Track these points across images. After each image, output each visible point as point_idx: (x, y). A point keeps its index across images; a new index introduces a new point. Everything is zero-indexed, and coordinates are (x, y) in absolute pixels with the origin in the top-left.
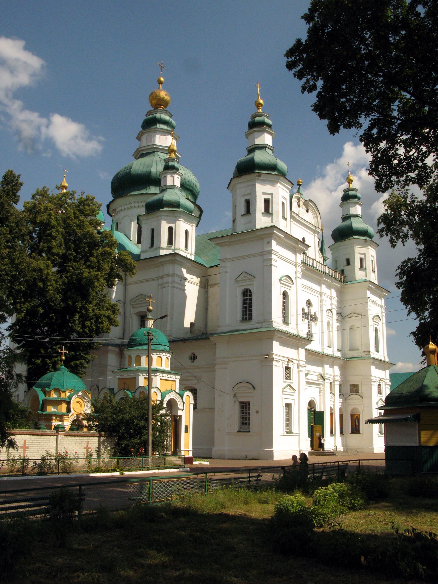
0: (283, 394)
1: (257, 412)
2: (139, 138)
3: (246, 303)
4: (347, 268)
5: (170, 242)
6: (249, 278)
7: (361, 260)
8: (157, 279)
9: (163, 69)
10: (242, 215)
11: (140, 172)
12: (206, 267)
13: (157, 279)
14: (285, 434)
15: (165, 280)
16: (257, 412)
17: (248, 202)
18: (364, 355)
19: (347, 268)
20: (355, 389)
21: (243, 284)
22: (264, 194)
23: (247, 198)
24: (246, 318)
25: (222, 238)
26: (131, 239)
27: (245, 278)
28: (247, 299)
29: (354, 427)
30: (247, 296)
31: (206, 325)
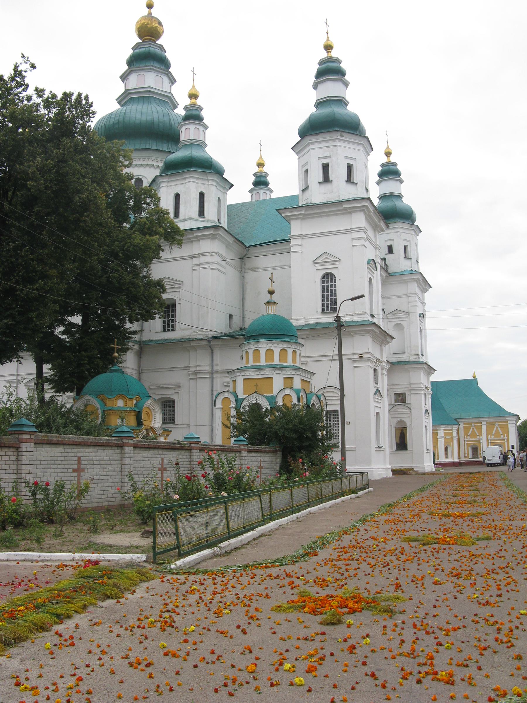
0: (375, 401)
2: (124, 77)
3: (327, 291)
4: (389, 257)
5: (202, 213)
6: (333, 260)
7: (405, 247)
8: (191, 258)
10: (320, 183)
11: (137, 122)
12: (245, 246)
13: (191, 258)
14: (377, 449)
15: (203, 259)
17: (326, 167)
18: (412, 359)
19: (389, 257)
20: (400, 398)
22: (346, 157)
23: (325, 161)
24: (328, 309)
25: (295, 209)
28: (327, 286)
31: (243, 318)
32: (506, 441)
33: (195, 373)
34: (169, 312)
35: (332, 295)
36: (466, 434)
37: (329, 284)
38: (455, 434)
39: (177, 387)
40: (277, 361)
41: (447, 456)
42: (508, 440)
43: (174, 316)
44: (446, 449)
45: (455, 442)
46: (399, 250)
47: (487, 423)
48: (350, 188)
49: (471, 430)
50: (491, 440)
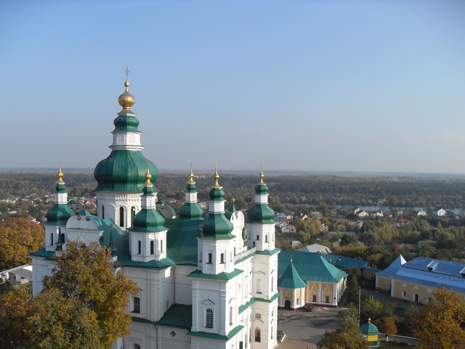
3: (209, 316)
5: (152, 252)
7: (266, 236)
9: (128, 72)
10: (207, 263)
11: (119, 175)
17: (210, 255)
18: (265, 298)
19: (257, 242)
20: (258, 316)
21: (207, 306)
24: (209, 325)
26: (116, 224)
27: (208, 303)
28: (209, 314)
30: (209, 312)
32: (331, 295)
34: (137, 301)
35: (211, 319)
36: (310, 288)
37: (210, 313)
41: (297, 304)
43: (139, 303)
44: (297, 299)
47: (322, 284)
49: (313, 287)
50: (323, 293)
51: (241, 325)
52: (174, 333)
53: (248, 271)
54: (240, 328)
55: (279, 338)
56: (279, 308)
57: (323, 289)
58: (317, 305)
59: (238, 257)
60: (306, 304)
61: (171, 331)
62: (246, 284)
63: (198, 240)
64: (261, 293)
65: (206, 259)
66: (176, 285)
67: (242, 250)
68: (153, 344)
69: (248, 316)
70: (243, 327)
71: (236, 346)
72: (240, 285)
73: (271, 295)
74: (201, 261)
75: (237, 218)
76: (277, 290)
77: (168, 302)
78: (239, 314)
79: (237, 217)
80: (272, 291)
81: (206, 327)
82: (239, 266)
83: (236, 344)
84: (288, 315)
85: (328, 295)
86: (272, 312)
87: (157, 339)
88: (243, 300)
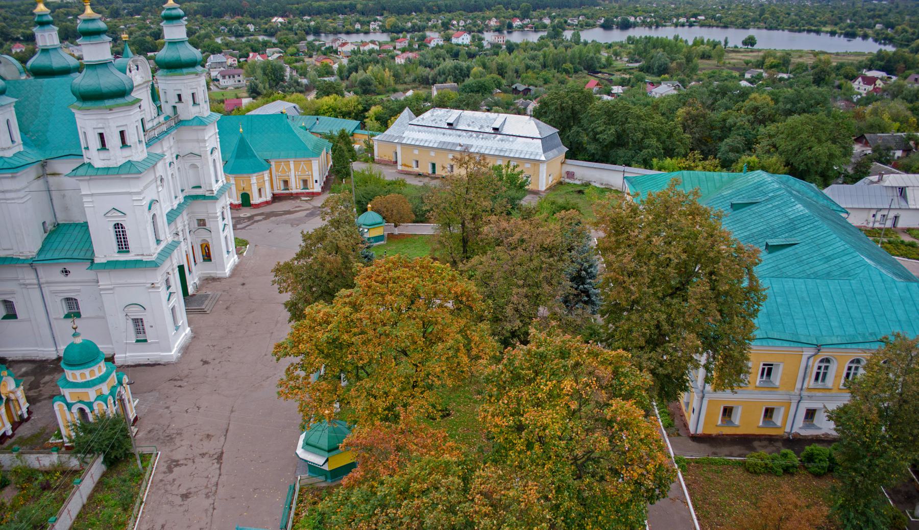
1: (152, 327)
4: (178, 105)
7: (193, 94)
15: (8, 195)
16: (152, 327)
18: (207, 194)
19: (179, 105)
22: (117, 127)
29: (204, 254)
31: (55, 215)
33: (26, 285)
36: (277, 171)
37: (121, 230)
38: (267, 178)
39: (13, 293)
40: (89, 378)
41: (260, 196)
42: (312, 175)
44: (260, 190)
45: (267, 185)
46: (187, 98)
48: (126, 152)
51: (176, 239)
52: (66, 272)
53: (172, 154)
54: (174, 245)
55: (239, 253)
56: (233, 206)
57: (296, 169)
58: (291, 194)
59: (152, 134)
60: (273, 194)
61: (61, 269)
62: (172, 174)
63: (73, 114)
64: (200, 187)
65: (95, 143)
66: (53, 193)
67: (155, 122)
68: (36, 293)
69: (184, 226)
70: (179, 243)
71: (174, 274)
72: (162, 180)
73: (216, 187)
74: (87, 148)
75: (138, 69)
76: (224, 179)
77: (44, 223)
78: (169, 224)
79: (137, 66)
80: (217, 181)
81: (119, 252)
82: (157, 150)
83: (173, 270)
84: (248, 215)
85: (305, 177)
86: (223, 213)
87: (40, 285)
88: (172, 203)
